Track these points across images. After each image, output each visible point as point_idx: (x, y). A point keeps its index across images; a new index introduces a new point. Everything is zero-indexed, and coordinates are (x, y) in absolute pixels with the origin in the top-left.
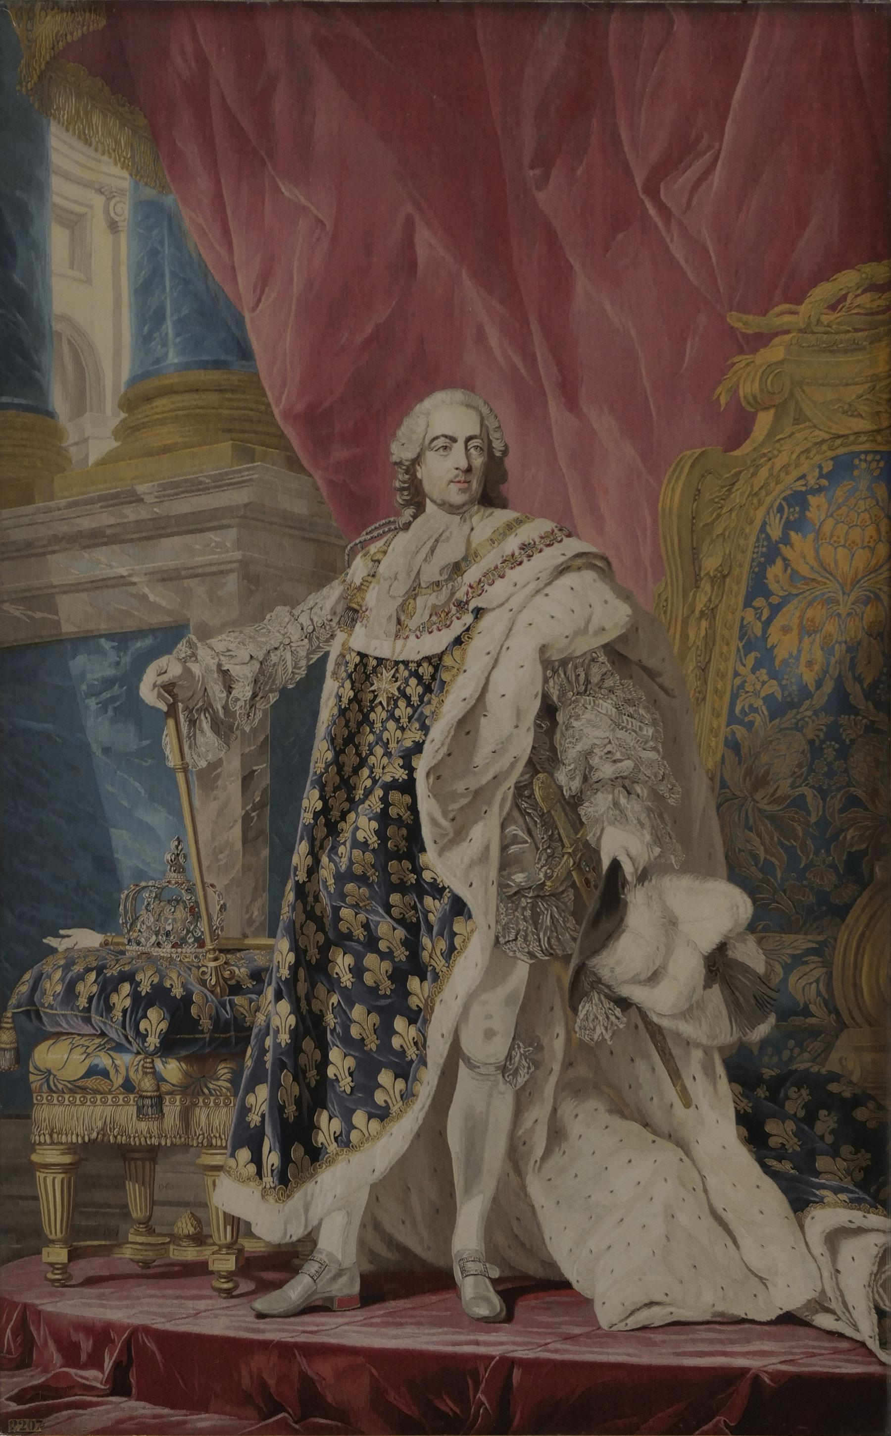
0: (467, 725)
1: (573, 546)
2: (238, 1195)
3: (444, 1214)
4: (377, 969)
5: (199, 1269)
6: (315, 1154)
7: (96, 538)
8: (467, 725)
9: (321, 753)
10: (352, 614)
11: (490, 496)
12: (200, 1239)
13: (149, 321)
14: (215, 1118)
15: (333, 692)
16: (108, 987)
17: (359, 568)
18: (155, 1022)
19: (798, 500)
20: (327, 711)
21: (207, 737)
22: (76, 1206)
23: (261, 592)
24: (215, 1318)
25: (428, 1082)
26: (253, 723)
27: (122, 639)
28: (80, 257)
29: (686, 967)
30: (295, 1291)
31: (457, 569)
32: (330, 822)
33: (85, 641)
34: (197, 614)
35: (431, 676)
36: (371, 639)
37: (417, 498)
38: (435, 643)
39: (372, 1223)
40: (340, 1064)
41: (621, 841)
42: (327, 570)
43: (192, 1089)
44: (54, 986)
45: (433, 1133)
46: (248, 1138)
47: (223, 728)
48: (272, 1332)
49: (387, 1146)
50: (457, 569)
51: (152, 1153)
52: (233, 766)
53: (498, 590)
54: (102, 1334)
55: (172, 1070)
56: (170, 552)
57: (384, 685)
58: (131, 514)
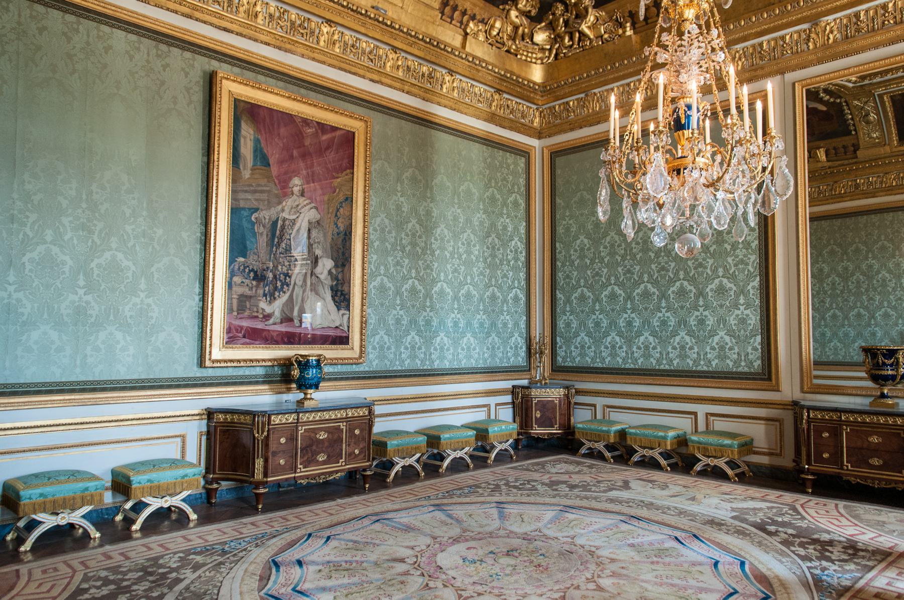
0: (298, 231)
1: (313, 205)
2: (263, 305)
3: (292, 310)
4: (285, 269)
5: (257, 317)
6: (275, 298)
7: (246, 191)
8: (298, 231)
9: (278, 232)
10: (283, 210)
11: (302, 194)
12: (257, 312)
13: (255, 157)
14: (261, 292)
15: (280, 223)
16: (245, 268)
17: (284, 203)
18: (252, 275)
19: (341, 203)
20: (279, 226)
21: (262, 227)
22: (238, 306)
23: (269, 206)
24: (259, 325)
25: (291, 287)
26: (268, 226)
27: (250, 209)
28: (245, 144)
29: (326, 272)
30: (271, 321)
31: (298, 206)
32: (279, 244)
33: (244, 209)
34: (261, 207)
35: (294, 222)
36: (285, 215)
37: (293, 194)
38: (294, 217)
39: (283, 311)
40: (279, 284)
41: (318, 252)
42: (280, 203)
43: (257, 286)
44: (237, 267)
45: (291, 296)
46: (265, 295)
47: (264, 226)
48: (267, 328)
49: (285, 297)
50: (298, 206)
51: (251, 297)
52: (265, 233)
53: (303, 210)
54: (242, 327)
55: (254, 283)
56: (257, 196)
57: (287, 223)
58: (252, 188)
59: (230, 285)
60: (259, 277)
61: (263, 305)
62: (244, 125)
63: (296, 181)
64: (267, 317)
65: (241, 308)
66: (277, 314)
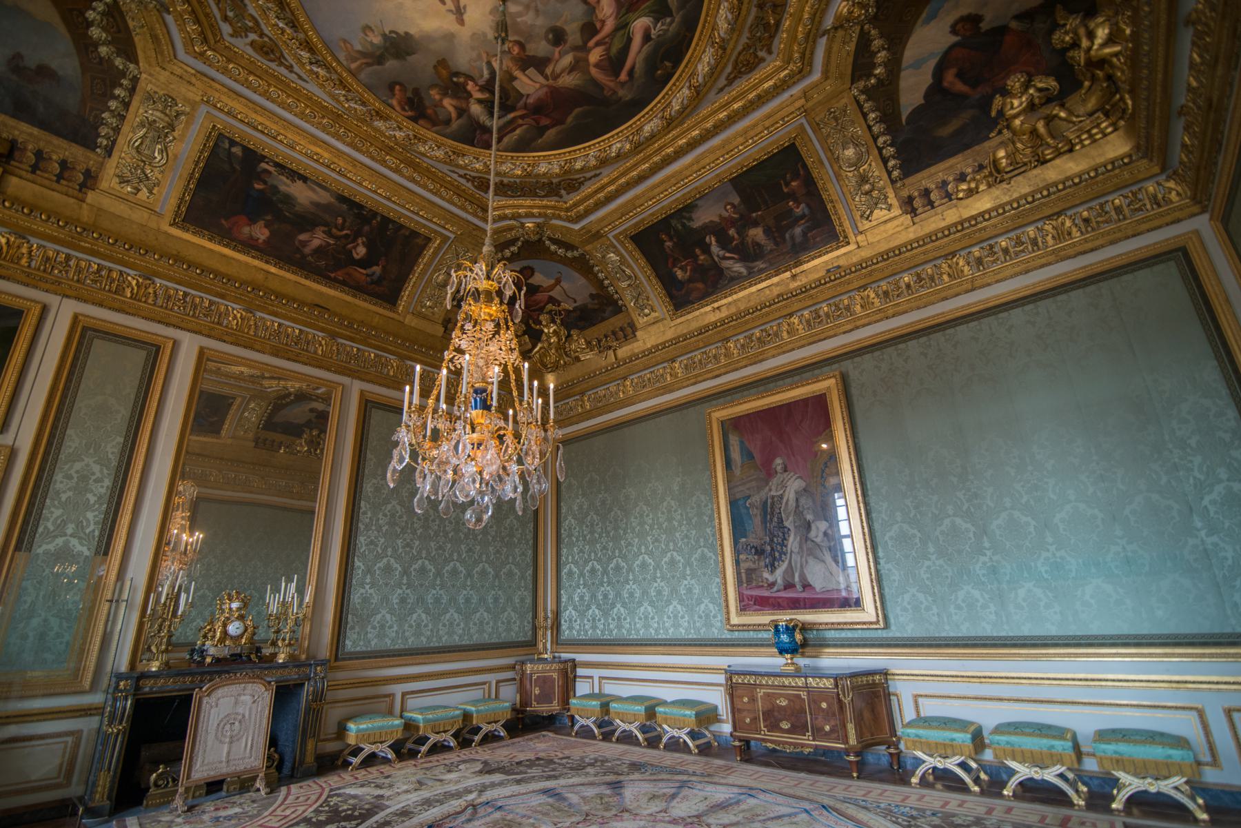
2: (766, 575)
14: (762, 564)
23: (759, 489)
24: (766, 593)
30: (775, 589)
35: (781, 497)
36: (773, 493)
40: (777, 554)
45: (790, 562)
46: (766, 566)
49: (784, 566)
56: (748, 486)
59: (737, 562)
60: (759, 552)
61: (766, 575)
62: (731, 436)
63: (779, 461)
64: (772, 585)
65: (749, 581)
66: (780, 581)
